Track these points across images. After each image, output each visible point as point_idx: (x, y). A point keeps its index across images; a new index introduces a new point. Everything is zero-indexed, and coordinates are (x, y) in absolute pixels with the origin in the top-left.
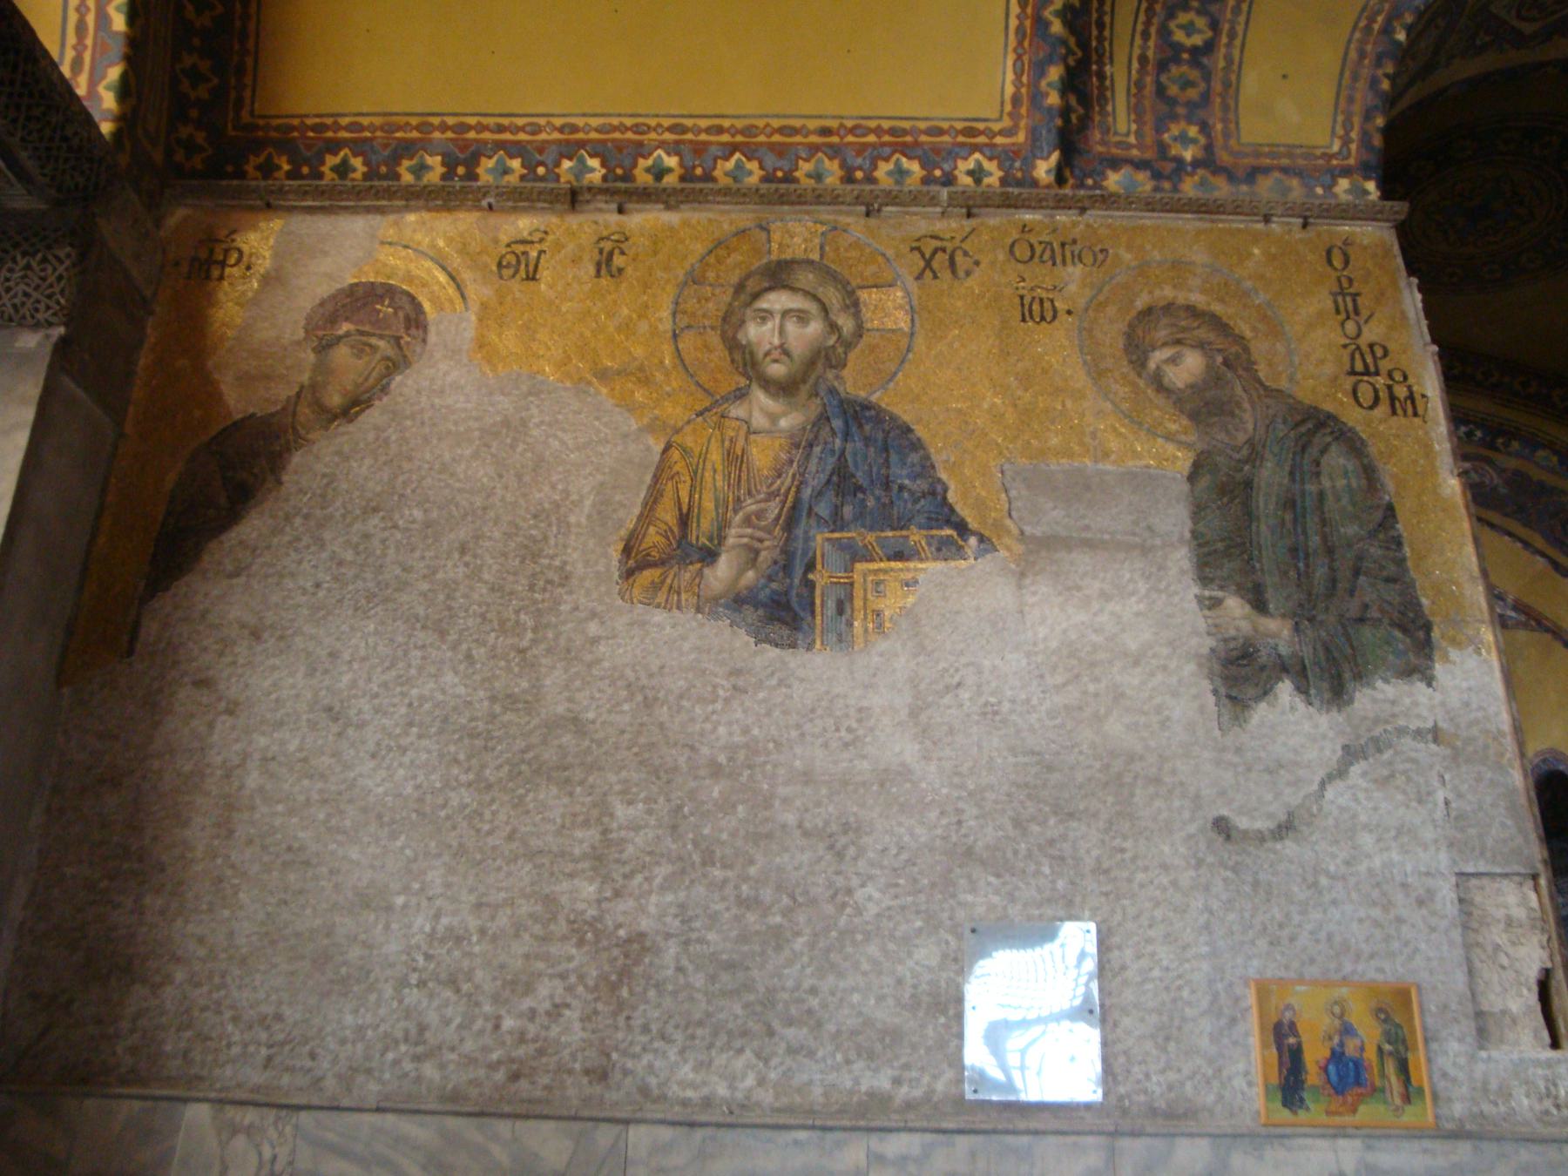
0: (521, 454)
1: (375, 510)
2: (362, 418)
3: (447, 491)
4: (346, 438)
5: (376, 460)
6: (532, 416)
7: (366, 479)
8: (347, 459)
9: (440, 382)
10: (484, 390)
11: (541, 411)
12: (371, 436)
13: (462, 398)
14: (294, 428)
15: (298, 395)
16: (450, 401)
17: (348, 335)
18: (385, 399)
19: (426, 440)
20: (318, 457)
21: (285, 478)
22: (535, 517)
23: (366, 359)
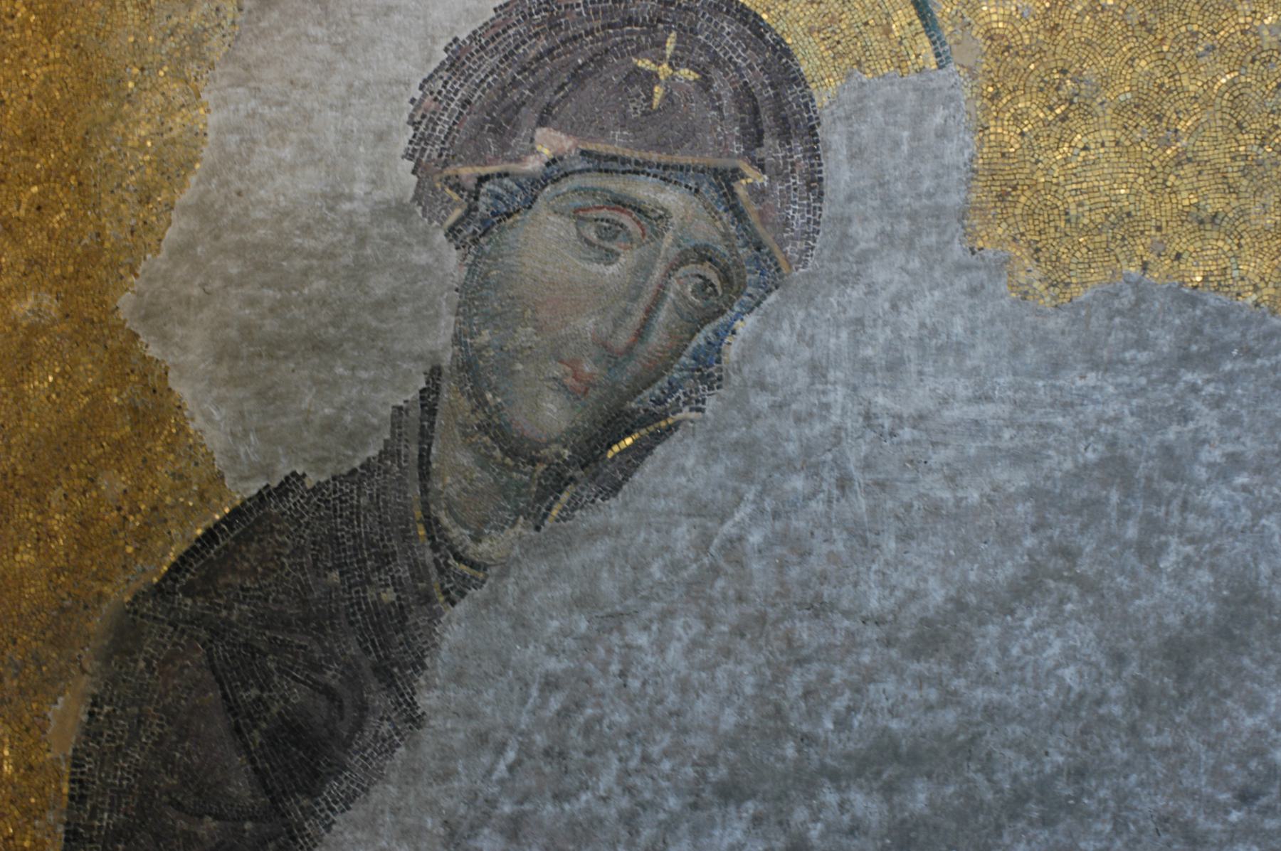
0: (1178, 577)
1: (730, 793)
2: (646, 474)
3: (949, 717)
4: (600, 550)
5: (709, 621)
6: (1199, 442)
7: (684, 687)
8: (616, 621)
9: (884, 335)
10: (1031, 355)
11: (1231, 421)
12: (683, 535)
13: (963, 388)
14: (431, 523)
15: (428, 401)
16: (920, 398)
17: (556, 171)
18: (711, 403)
19: (862, 537)
20: (521, 623)
21: (427, 700)
22: (1245, 797)
23: (627, 259)
